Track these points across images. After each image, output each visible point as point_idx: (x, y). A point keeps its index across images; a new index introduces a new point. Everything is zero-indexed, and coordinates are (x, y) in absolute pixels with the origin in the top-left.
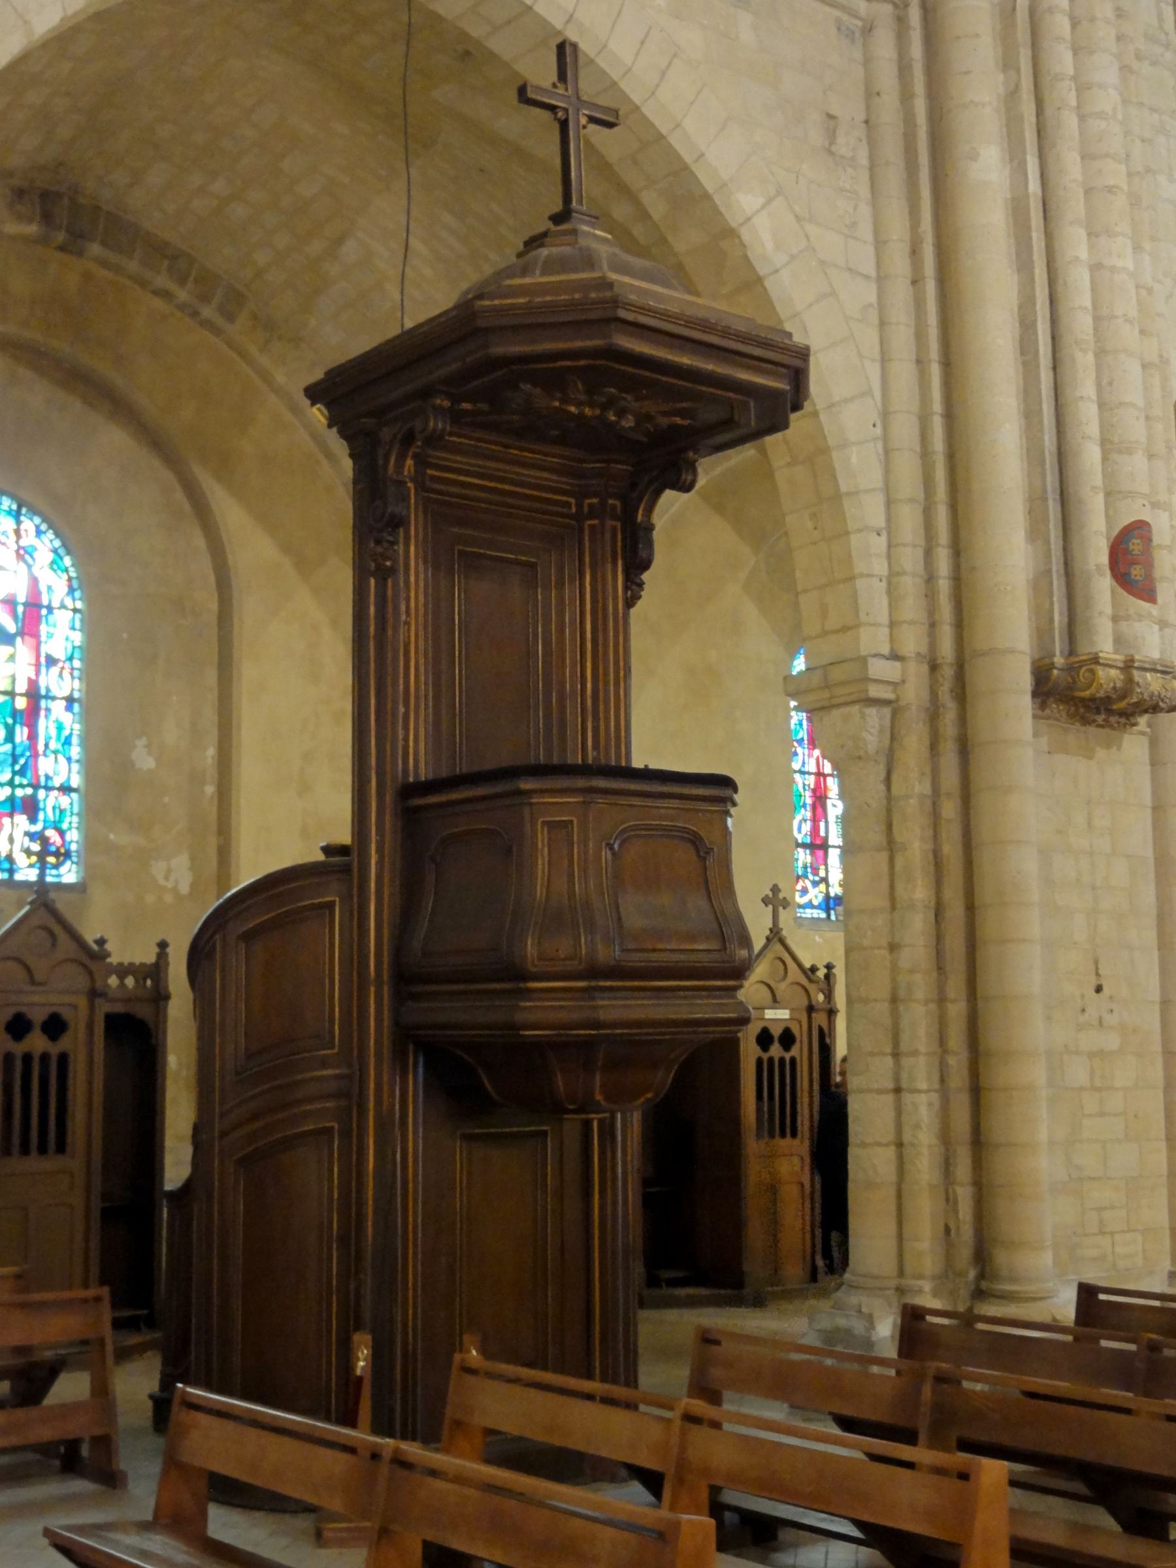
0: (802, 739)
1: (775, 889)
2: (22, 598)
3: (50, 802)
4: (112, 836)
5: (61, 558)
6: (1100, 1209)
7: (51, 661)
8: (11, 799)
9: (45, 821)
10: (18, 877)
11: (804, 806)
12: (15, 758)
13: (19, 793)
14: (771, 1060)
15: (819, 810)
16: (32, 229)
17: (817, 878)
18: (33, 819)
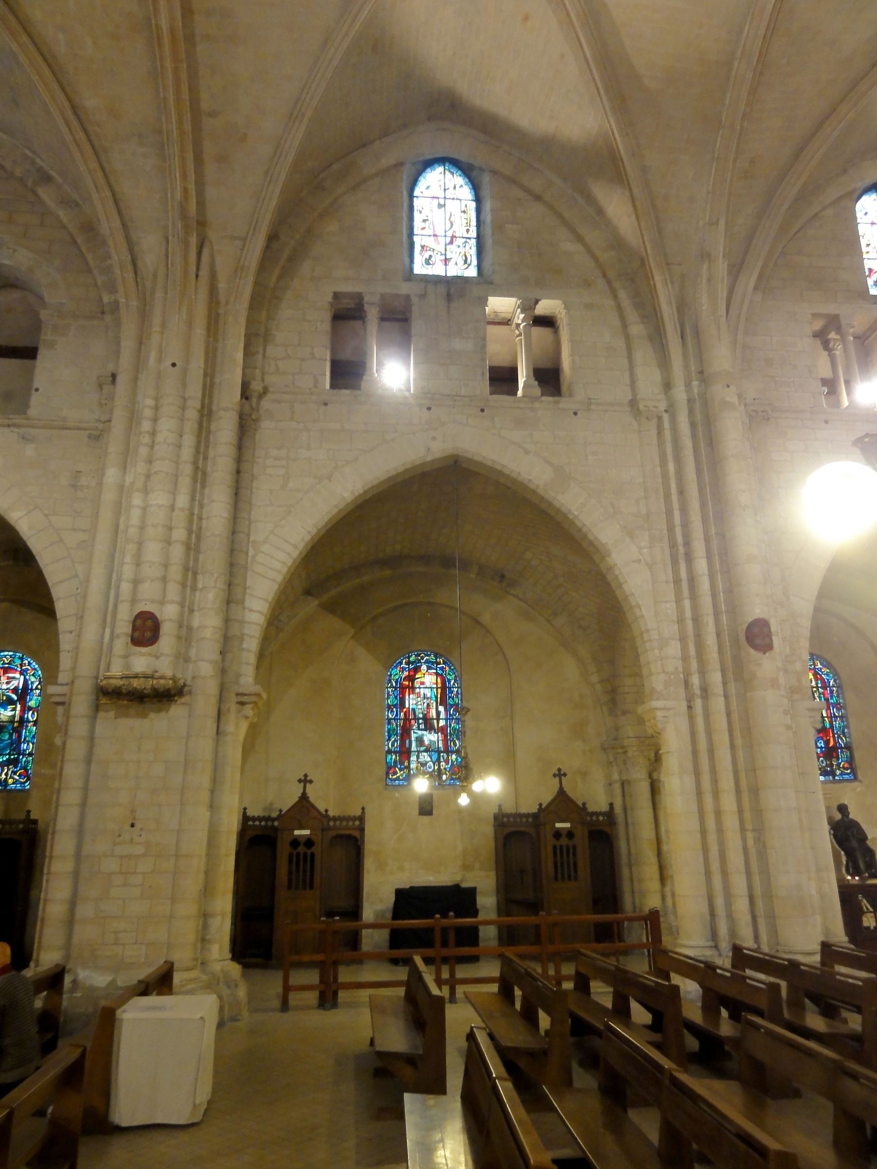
0: (397, 704)
1: (306, 776)
2: (21, 687)
3: (24, 759)
4: (43, 771)
5: (38, 671)
6: (116, 932)
7: (30, 709)
8: (8, 760)
9: (20, 767)
10: (8, 788)
11: (397, 734)
12: (11, 744)
13: (12, 757)
14: (298, 854)
15: (405, 735)
16: (11, 562)
17: (402, 767)
18: (16, 767)
